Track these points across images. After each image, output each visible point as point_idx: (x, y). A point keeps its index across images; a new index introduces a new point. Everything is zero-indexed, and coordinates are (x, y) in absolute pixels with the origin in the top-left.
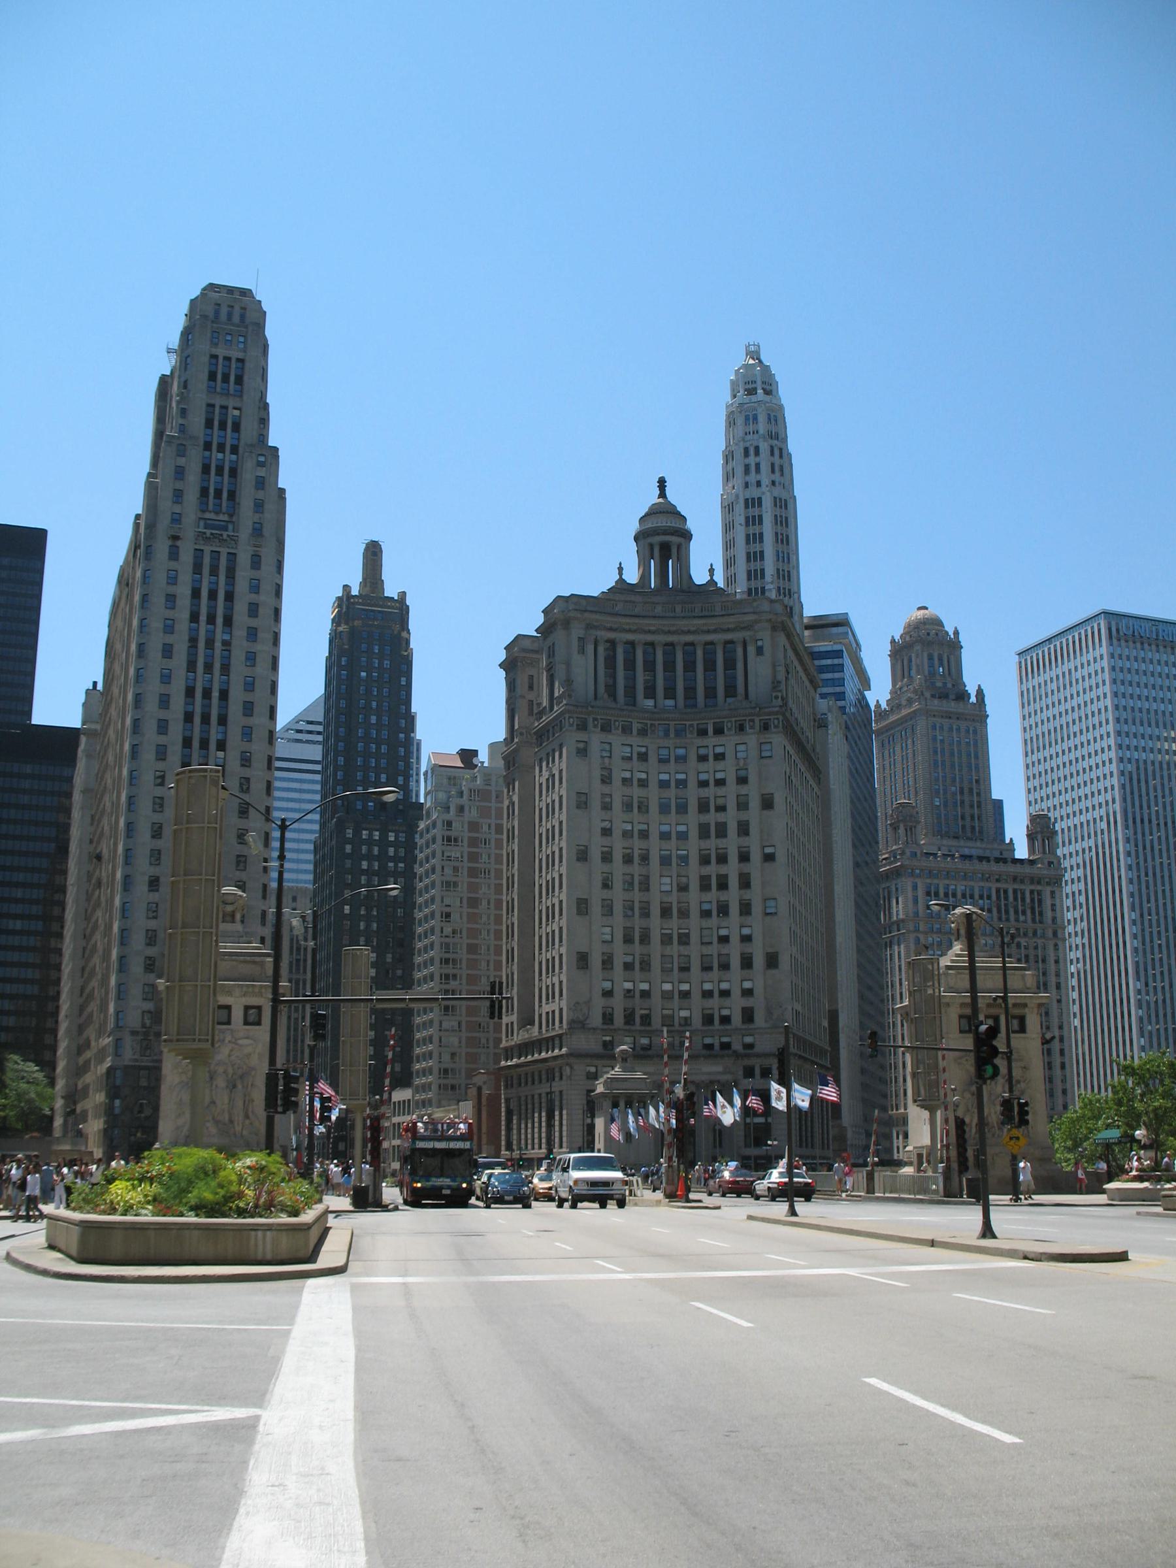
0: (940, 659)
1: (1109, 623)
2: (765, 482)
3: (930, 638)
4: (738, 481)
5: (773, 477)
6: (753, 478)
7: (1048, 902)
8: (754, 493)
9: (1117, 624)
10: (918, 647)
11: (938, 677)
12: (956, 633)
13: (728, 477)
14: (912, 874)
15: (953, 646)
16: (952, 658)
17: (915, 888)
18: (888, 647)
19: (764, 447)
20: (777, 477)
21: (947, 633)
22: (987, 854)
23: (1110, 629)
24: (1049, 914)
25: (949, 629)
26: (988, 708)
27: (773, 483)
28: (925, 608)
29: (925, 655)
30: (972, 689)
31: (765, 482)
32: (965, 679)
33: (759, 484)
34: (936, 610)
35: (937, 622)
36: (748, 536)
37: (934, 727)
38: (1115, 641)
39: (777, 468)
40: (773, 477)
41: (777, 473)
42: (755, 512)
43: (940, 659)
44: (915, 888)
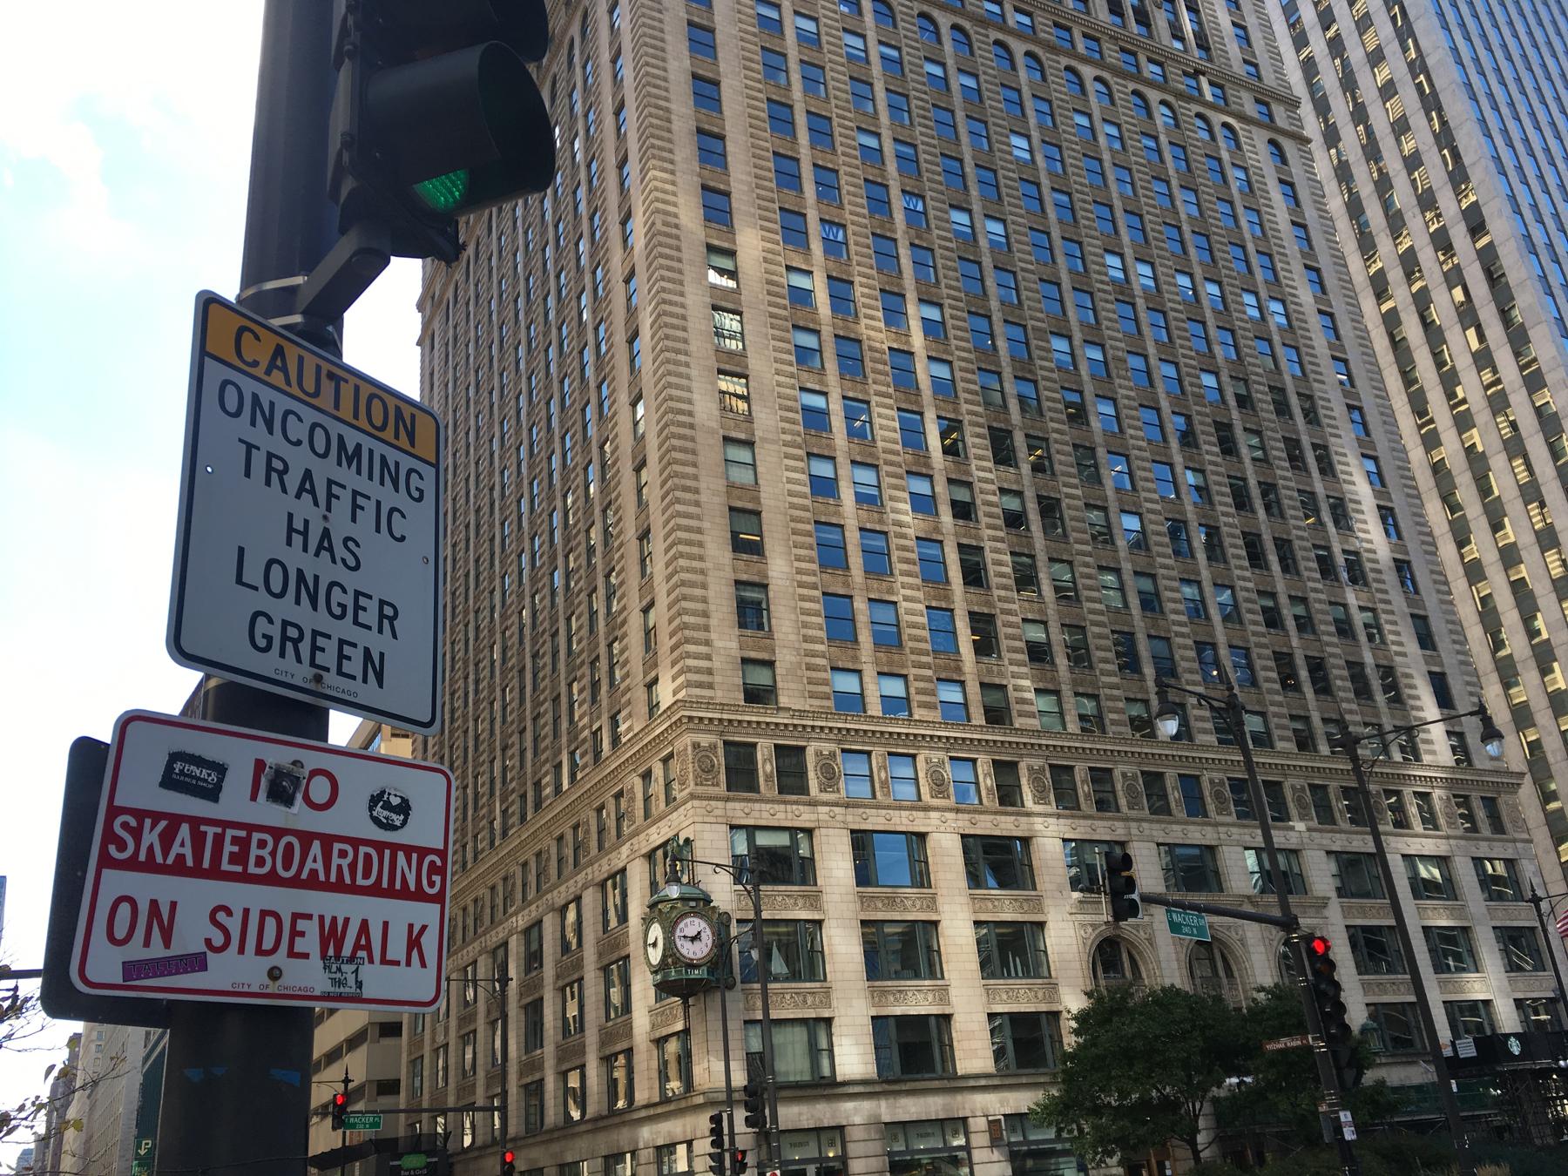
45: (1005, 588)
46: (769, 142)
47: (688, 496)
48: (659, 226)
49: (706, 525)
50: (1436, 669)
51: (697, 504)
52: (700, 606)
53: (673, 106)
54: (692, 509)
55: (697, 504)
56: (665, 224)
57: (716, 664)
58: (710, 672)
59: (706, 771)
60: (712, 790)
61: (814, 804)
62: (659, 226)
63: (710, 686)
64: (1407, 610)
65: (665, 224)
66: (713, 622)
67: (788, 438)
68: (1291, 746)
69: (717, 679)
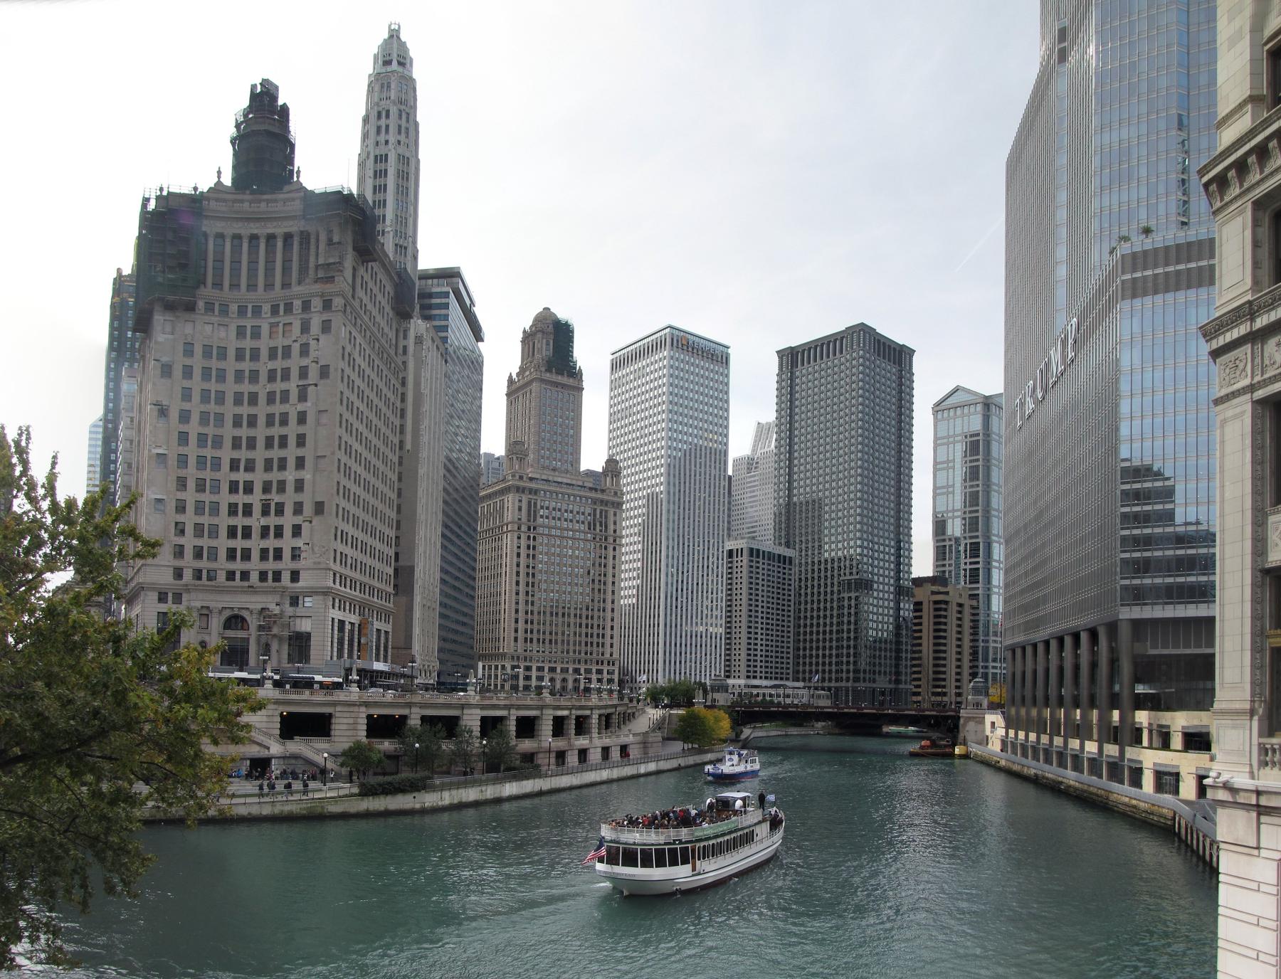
2: (392, 139)
4: (371, 142)
5: (399, 138)
6: (382, 138)
7: (611, 518)
8: (382, 150)
13: (365, 136)
19: (394, 111)
20: (402, 138)
24: (611, 527)
27: (399, 142)
31: (392, 139)
33: (387, 142)
36: (375, 187)
39: (403, 130)
40: (399, 138)
41: (403, 135)
42: (381, 166)
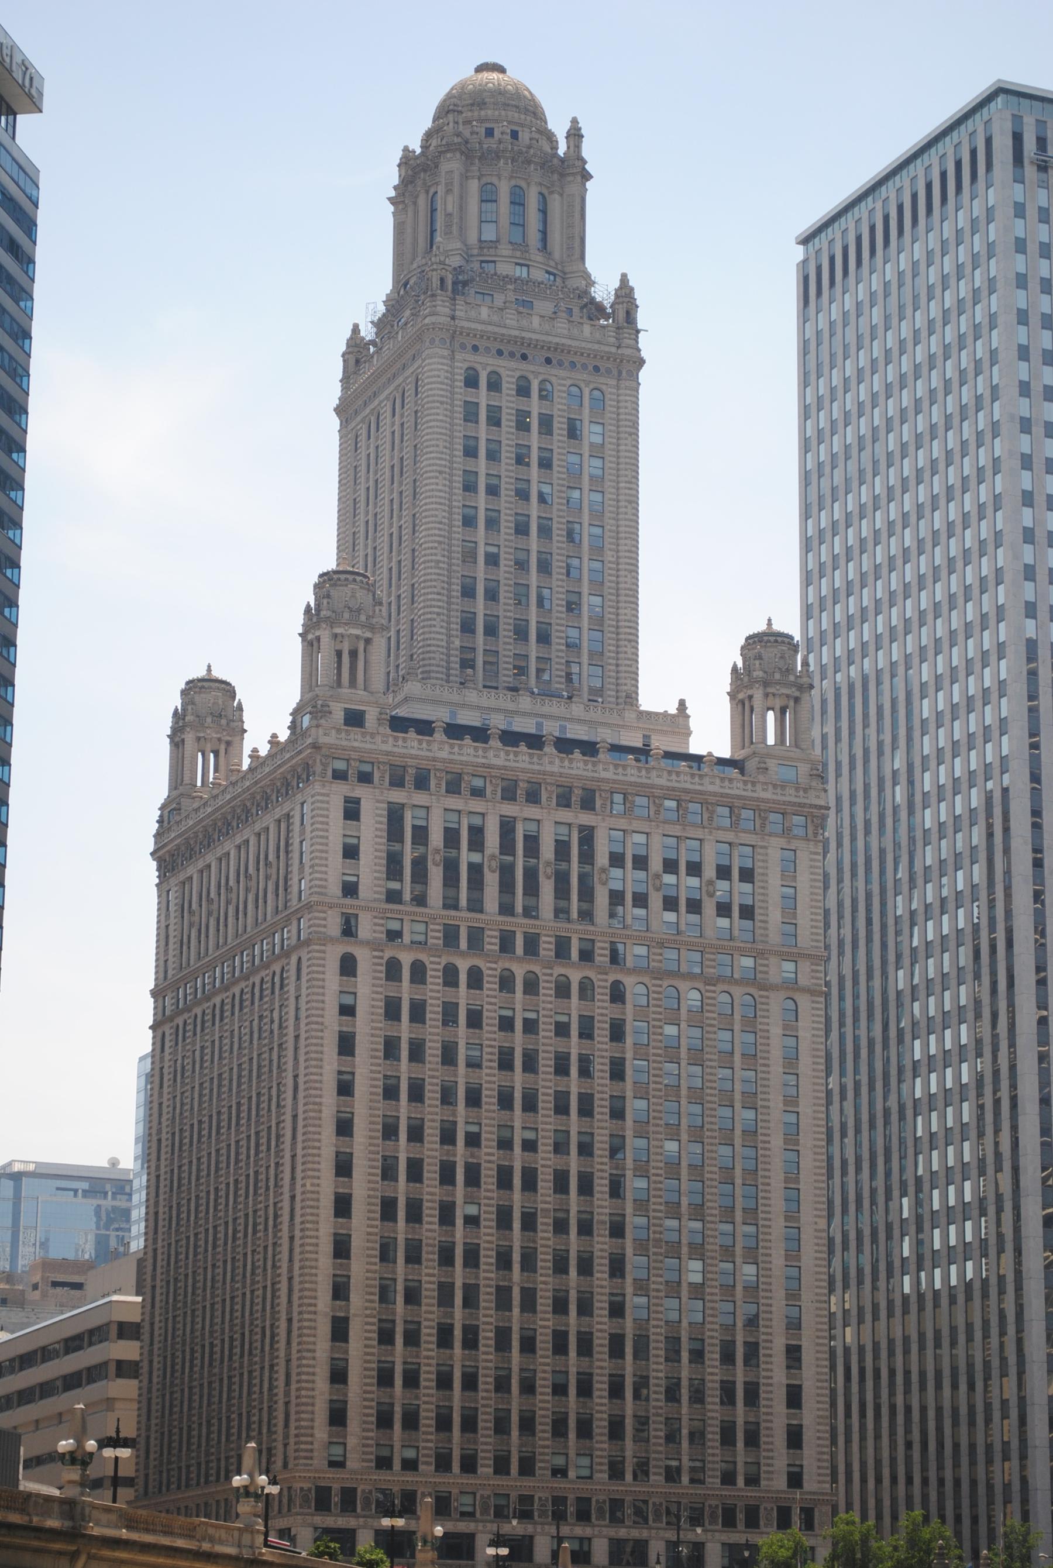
0: (518, 201)
1: (1017, 119)
3: (491, 143)
9: (1041, 124)
10: (452, 165)
11: (505, 250)
12: (575, 134)
14: (340, 776)
15: (569, 172)
16: (555, 204)
17: (352, 812)
18: (394, 177)
21: (550, 137)
22: (605, 736)
23: (1017, 138)
25: (558, 126)
26: (644, 342)
28: (502, 70)
29: (474, 186)
30: (604, 291)
32: (593, 264)
34: (524, 73)
35: (524, 109)
37: (472, 381)
38: (1030, 171)
43: (518, 201)
44: (352, 812)
45: (487, 1391)
46: (382, 1106)
47: (309, 1355)
48: (309, 1187)
49: (317, 1370)
50: (795, 1422)
51: (314, 1358)
52: (309, 1416)
53: (324, 1100)
54: (311, 1362)
55: (314, 1358)
56: (312, 1185)
57: (316, 1446)
58: (312, 1451)
59: (306, 1500)
60: (306, 1511)
61: (358, 1517)
62: (309, 1187)
63: (311, 1458)
64: (785, 1381)
65: (312, 1185)
66: (316, 1424)
67: (368, 1312)
68: (661, 1479)
69: (316, 1454)
